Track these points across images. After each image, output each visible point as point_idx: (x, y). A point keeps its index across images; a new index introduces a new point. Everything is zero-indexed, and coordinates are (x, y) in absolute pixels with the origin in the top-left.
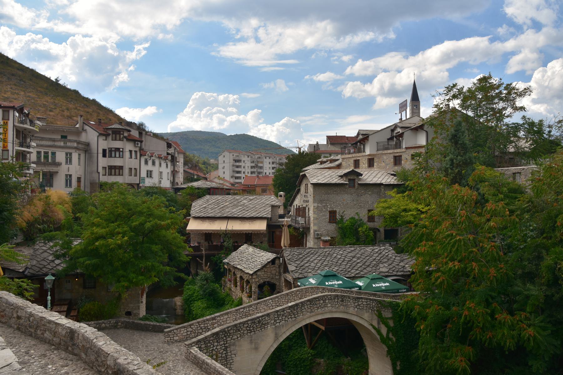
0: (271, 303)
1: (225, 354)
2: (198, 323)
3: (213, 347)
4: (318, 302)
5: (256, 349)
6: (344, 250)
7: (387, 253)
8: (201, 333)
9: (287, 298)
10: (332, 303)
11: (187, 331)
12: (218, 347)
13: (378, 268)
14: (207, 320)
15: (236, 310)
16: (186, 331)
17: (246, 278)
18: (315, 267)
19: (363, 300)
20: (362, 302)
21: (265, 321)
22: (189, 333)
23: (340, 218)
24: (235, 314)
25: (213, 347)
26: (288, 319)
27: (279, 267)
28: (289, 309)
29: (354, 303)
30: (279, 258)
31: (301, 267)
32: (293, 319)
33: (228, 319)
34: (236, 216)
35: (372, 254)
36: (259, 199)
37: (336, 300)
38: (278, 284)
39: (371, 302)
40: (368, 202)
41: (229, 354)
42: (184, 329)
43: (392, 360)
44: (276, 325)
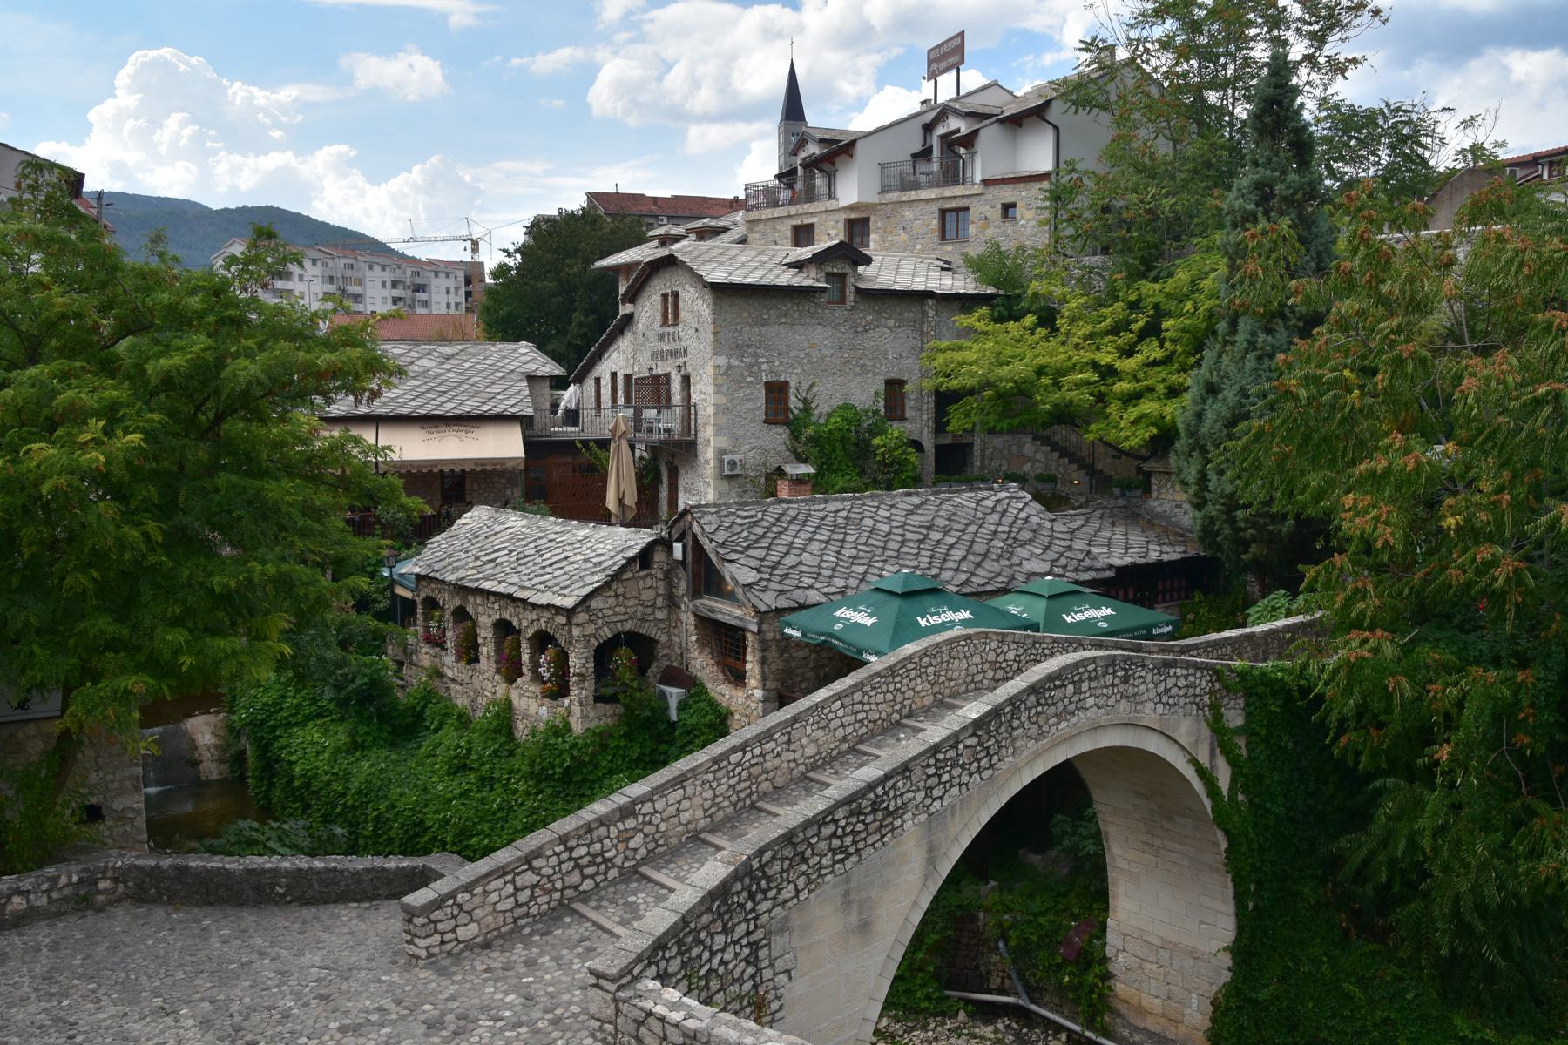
0: (840, 713)
1: (753, 977)
2: (563, 840)
3: (709, 961)
4: (1057, 694)
5: (864, 927)
6: (892, 506)
7: (1021, 510)
8: (576, 887)
9: (891, 687)
10: (1098, 692)
11: (516, 890)
12: (726, 953)
13: (1016, 560)
14: (602, 821)
15: (715, 761)
16: (510, 888)
17: (528, 624)
18: (819, 567)
19: (1179, 670)
20: (1174, 680)
21: (895, 797)
22: (524, 896)
23: (801, 405)
24: (710, 777)
25: (709, 961)
26: (971, 775)
27: (668, 576)
28: (974, 734)
29: (1156, 685)
30: (666, 544)
31: (773, 568)
32: (986, 774)
33: (686, 804)
34: (404, 411)
35: (979, 515)
36: (474, 355)
37: (1109, 679)
38: (663, 639)
39: (1199, 674)
40: (885, 353)
41: (767, 974)
42: (501, 881)
43: (1238, 882)
44: (932, 809)
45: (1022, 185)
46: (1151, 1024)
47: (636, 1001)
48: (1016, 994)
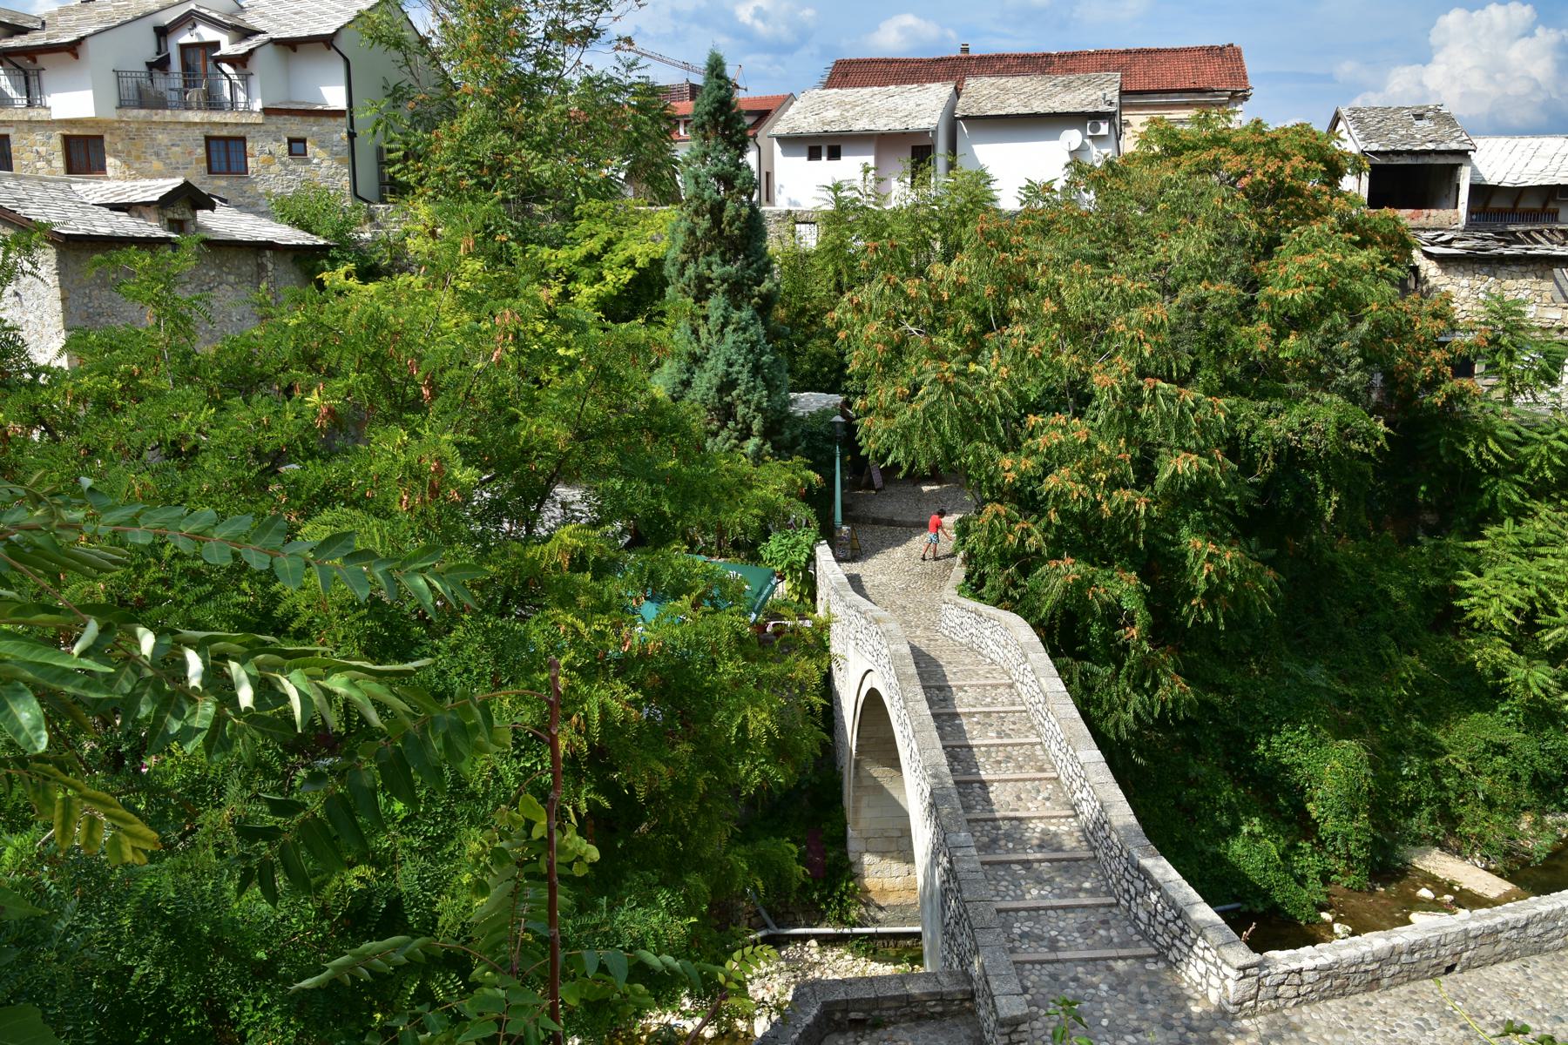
45: (312, 119)
46: (892, 900)
48: (766, 926)
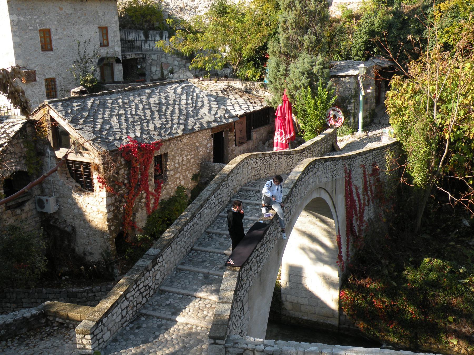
8: (140, 303)
47: (237, 345)
